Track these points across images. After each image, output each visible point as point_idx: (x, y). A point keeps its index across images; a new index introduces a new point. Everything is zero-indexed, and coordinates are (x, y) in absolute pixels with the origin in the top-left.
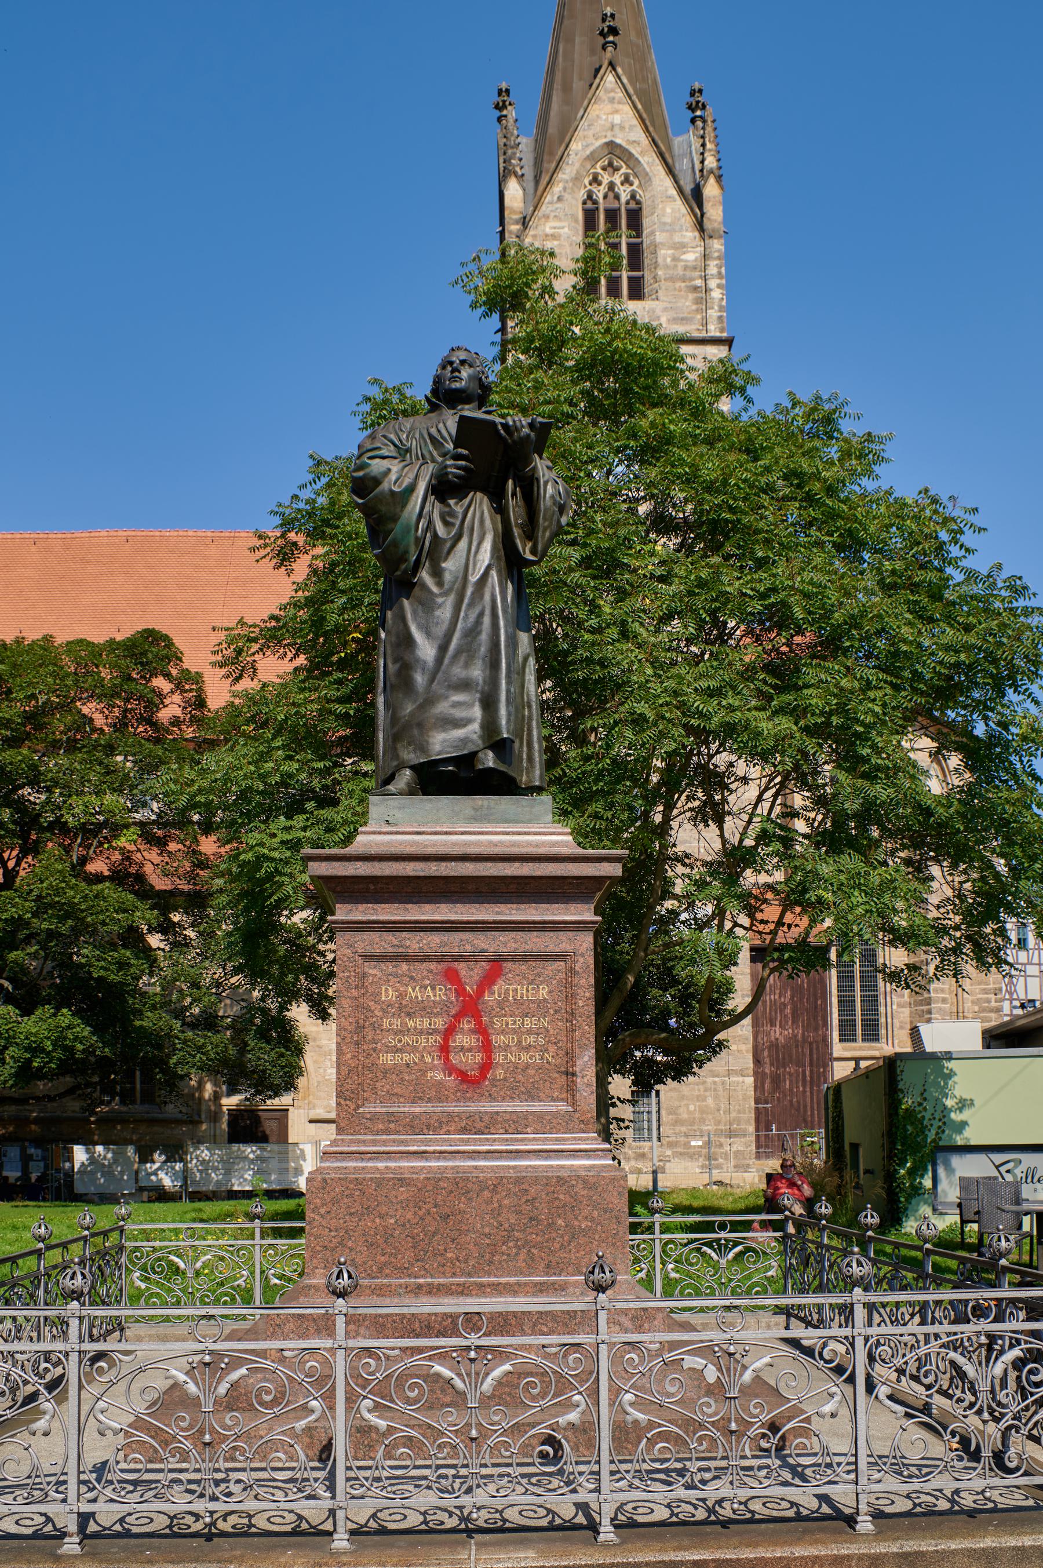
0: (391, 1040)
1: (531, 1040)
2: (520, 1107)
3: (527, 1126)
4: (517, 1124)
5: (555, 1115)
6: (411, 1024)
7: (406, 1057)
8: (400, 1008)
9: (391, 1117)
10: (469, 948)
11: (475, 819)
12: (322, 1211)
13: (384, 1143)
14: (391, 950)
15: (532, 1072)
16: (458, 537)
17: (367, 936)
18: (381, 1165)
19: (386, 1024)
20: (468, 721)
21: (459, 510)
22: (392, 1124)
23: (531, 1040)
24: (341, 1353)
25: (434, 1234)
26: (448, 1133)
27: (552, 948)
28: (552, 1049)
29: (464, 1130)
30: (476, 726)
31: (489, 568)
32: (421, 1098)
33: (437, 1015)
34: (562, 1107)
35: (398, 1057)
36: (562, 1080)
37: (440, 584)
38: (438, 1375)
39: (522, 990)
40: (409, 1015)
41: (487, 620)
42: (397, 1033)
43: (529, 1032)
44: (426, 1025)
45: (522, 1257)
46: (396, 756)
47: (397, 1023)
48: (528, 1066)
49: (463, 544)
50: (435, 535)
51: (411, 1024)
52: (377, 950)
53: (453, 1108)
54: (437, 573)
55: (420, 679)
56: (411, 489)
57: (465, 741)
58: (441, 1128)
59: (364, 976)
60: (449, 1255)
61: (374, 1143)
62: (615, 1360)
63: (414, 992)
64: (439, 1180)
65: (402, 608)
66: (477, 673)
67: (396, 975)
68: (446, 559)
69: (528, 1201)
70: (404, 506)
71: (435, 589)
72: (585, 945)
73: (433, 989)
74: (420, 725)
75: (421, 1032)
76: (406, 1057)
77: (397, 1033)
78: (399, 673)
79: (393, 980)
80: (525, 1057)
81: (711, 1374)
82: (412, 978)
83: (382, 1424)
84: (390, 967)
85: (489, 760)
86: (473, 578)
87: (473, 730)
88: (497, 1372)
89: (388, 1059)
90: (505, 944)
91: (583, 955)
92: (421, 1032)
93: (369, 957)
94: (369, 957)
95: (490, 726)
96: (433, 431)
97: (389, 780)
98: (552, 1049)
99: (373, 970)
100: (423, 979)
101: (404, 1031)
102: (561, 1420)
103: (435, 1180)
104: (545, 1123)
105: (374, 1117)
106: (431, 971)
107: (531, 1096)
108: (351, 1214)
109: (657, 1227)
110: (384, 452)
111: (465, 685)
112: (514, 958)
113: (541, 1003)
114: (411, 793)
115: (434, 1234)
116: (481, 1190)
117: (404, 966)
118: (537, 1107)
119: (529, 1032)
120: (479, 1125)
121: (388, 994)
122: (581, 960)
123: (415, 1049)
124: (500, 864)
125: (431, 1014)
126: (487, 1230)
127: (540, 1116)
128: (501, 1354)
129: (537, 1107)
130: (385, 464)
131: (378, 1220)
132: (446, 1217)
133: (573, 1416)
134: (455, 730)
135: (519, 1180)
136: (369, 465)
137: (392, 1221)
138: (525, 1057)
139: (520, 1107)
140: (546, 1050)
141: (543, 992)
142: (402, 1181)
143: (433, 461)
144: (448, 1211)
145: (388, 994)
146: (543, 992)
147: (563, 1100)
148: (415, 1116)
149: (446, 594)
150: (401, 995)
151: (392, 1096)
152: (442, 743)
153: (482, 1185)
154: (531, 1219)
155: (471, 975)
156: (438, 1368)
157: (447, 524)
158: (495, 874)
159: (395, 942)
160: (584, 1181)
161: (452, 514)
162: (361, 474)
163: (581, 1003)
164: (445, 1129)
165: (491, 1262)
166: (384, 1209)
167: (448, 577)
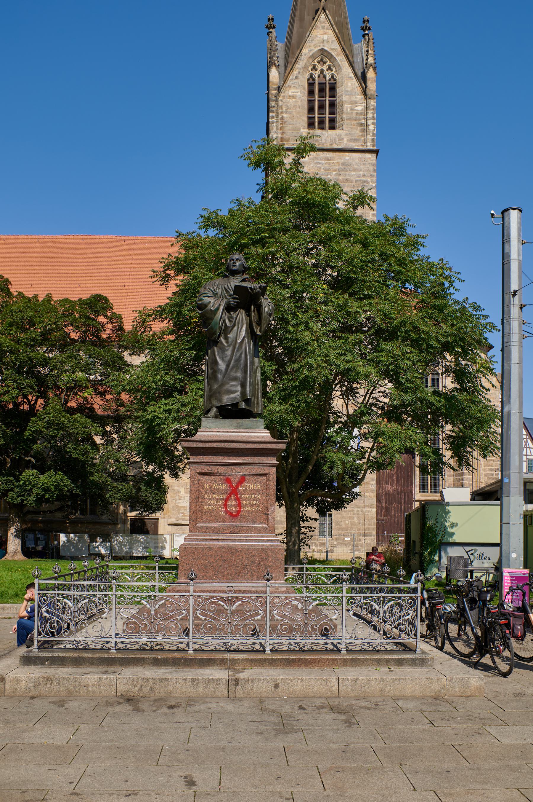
0: (208, 502)
1: (254, 502)
2: (250, 525)
4: (249, 531)
5: (261, 528)
6: (214, 496)
7: (213, 508)
9: (207, 527)
11: (238, 427)
13: (205, 536)
16: (234, 326)
17: (200, 467)
18: (203, 543)
19: (206, 497)
20: (236, 392)
21: (234, 316)
22: (207, 529)
23: (254, 502)
24: (191, 597)
28: (261, 506)
29: (231, 532)
30: (239, 393)
31: (244, 337)
33: (223, 494)
34: (264, 525)
35: (210, 507)
36: (264, 516)
37: (227, 342)
38: (220, 604)
39: (251, 486)
41: (243, 356)
42: (210, 499)
43: (254, 500)
44: (219, 497)
46: (211, 403)
47: (210, 496)
48: (253, 511)
49: (235, 328)
50: (226, 325)
51: (214, 496)
53: (227, 525)
54: (226, 338)
55: (220, 376)
56: (218, 309)
57: (235, 398)
59: (199, 480)
61: (202, 536)
62: (272, 600)
63: (215, 486)
65: (214, 350)
66: (239, 374)
70: (215, 314)
71: (225, 344)
74: (219, 393)
75: (218, 499)
76: (213, 508)
77: (210, 499)
78: (213, 373)
80: (252, 508)
81: (300, 606)
83: (203, 618)
84: (208, 477)
85: (243, 405)
86: (239, 341)
87: (237, 395)
88: (237, 604)
89: (207, 508)
93: (200, 474)
94: (200, 474)
95: (243, 393)
96: (226, 286)
97: (208, 411)
98: (261, 506)
99: (202, 478)
101: (212, 499)
102: (255, 618)
103: (221, 548)
104: (258, 531)
105: (202, 527)
107: (254, 521)
109: (305, 569)
110: (209, 295)
111: (235, 379)
112: (249, 475)
113: (258, 491)
114: (216, 417)
117: (213, 477)
118: (255, 525)
119: (254, 500)
120: (236, 531)
121: (207, 486)
123: (215, 505)
124: (245, 444)
125: (221, 493)
127: (256, 528)
128: (238, 599)
129: (255, 525)
130: (209, 299)
133: (259, 617)
134: (232, 395)
135: (249, 549)
136: (202, 300)
138: (252, 508)
139: (250, 525)
141: (259, 487)
142: (210, 549)
143: (226, 298)
145: (207, 486)
146: (259, 487)
148: (215, 527)
149: (229, 346)
150: (211, 487)
151: (207, 520)
152: (227, 399)
153: (236, 550)
155: (235, 480)
156: (220, 602)
157: (230, 321)
160: (270, 550)
161: (232, 317)
162: (200, 302)
165: (239, 576)
167: (230, 340)
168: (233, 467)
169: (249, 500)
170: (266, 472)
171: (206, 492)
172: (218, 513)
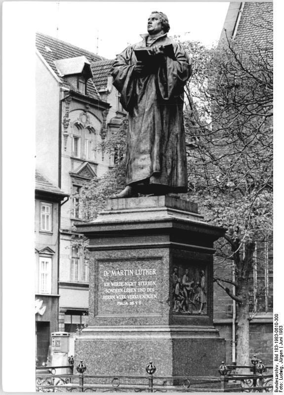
1: (150, 289)
3: (147, 322)
6: (112, 284)
8: (110, 278)
10: (130, 256)
12: (79, 352)
14: (106, 257)
15: (150, 302)
19: (105, 285)
25: (112, 361)
26: (122, 325)
27: (156, 255)
28: (157, 293)
32: (115, 312)
33: (121, 281)
40: (112, 281)
43: (149, 287)
44: (117, 285)
45: (139, 371)
47: (108, 284)
48: (148, 300)
51: (112, 284)
52: (101, 258)
58: (120, 323)
60: (116, 369)
64: (114, 341)
67: (108, 267)
68: (139, 102)
69: (141, 350)
72: (167, 253)
73: (120, 271)
79: (107, 268)
80: (148, 296)
82: (113, 267)
89: (105, 298)
90: (141, 254)
91: (165, 257)
92: (115, 288)
99: (101, 265)
100: (116, 268)
101: (111, 287)
105: (100, 319)
106: (119, 265)
108: (87, 354)
115: (112, 361)
116: (127, 346)
117: (111, 264)
122: (165, 259)
123: (114, 294)
125: (119, 281)
126: (128, 360)
131: (95, 356)
132: (115, 355)
137: (99, 356)
140: (155, 294)
141: (154, 272)
144: (116, 353)
146: (154, 272)
147: (160, 312)
154: (142, 357)
158: (133, 229)
159: (107, 254)
163: (165, 276)
164: (121, 323)
166: (97, 352)
167: (140, 109)
168: (128, 251)
169: (145, 287)
170: (160, 254)
171: (105, 280)
172: (116, 302)
